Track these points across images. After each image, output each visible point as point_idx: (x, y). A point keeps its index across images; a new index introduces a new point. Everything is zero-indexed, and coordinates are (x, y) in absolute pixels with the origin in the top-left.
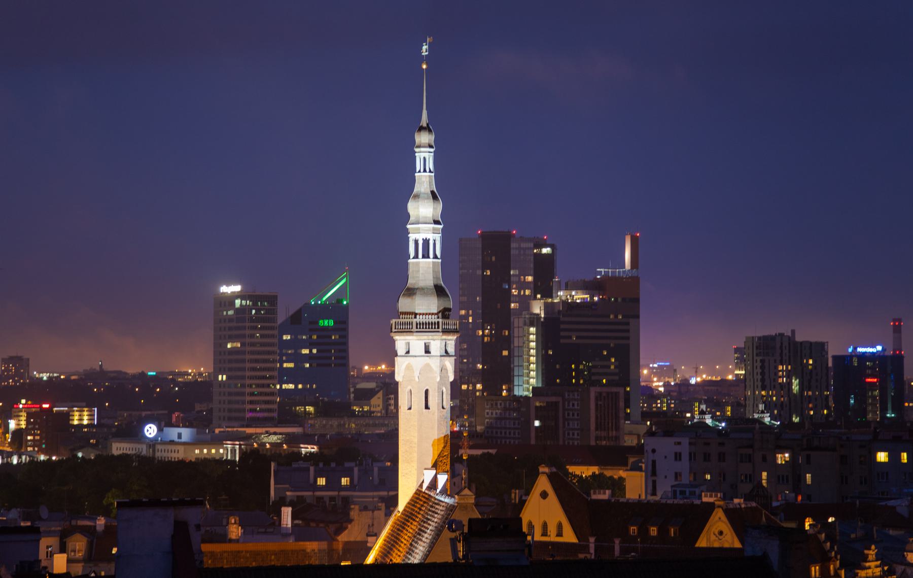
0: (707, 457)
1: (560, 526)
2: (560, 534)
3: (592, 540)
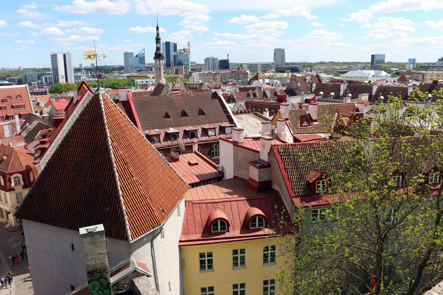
1: (180, 87)
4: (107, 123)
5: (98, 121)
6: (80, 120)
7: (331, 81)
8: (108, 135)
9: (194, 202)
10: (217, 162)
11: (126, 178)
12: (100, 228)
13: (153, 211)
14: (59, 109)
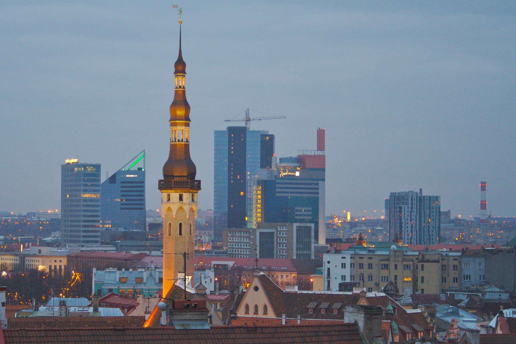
0: (361, 266)
1: (265, 307)
2: (265, 313)
3: (284, 317)
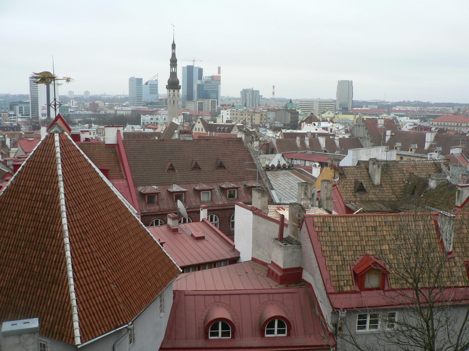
0: (234, 114)
1: (202, 129)
4: (63, 174)
5: (51, 170)
6: (26, 167)
7: (416, 128)
8: (62, 190)
9: (186, 293)
10: (231, 235)
11: (82, 254)
12: (34, 323)
13: (119, 303)
14: (28, 151)
